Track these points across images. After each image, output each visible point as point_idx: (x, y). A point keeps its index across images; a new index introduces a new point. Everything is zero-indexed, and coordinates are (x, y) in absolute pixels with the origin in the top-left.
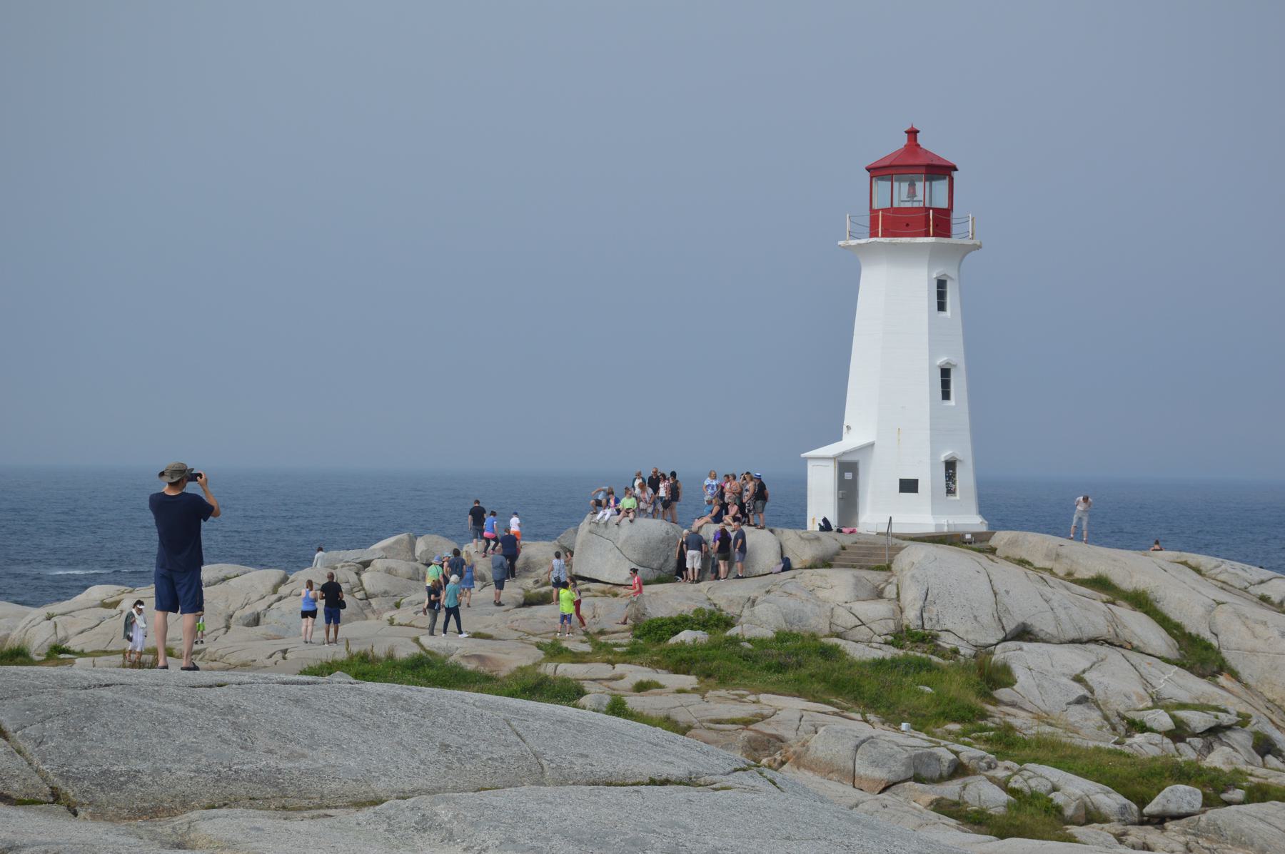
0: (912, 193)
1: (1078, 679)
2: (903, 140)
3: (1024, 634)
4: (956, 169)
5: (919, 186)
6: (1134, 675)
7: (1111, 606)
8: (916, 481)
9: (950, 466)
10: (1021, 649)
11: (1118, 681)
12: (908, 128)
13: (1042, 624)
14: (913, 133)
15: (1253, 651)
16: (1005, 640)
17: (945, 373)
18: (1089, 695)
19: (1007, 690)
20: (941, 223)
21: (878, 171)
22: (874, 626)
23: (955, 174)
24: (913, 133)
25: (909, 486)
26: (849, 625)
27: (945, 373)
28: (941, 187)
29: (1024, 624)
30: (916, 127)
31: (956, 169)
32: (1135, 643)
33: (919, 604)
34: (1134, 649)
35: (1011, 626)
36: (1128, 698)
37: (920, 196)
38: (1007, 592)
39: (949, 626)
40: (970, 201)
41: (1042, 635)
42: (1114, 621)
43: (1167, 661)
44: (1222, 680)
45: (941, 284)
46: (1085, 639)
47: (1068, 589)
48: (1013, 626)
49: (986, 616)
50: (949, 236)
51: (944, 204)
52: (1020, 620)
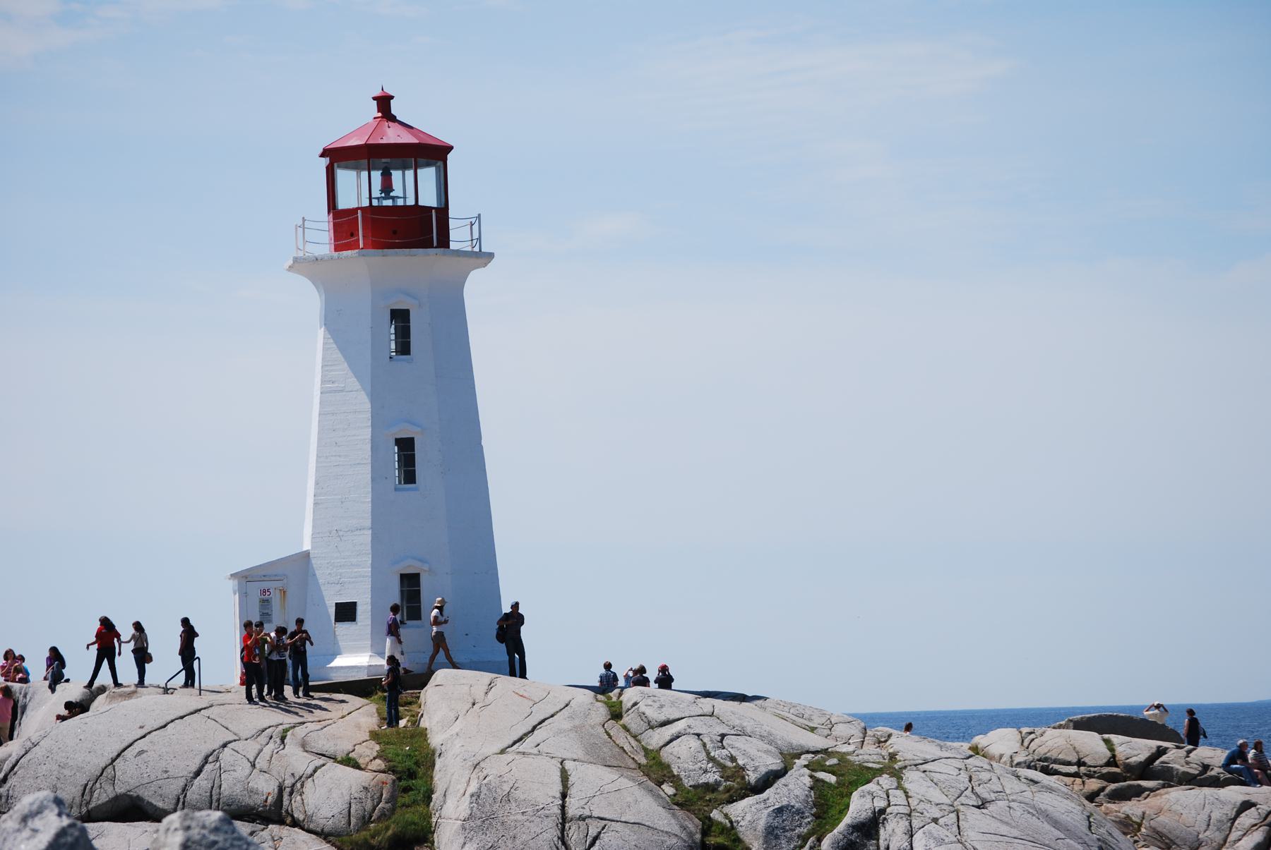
0: (387, 187)
2: (373, 110)
4: (449, 148)
5: (396, 175)
8: (354, 604)
12: (378, 93)
14: (384, 102)
17: (406, 447)
24: (384, 102)
25: (346, 612)
27: (406, 447)
28: (428, 175)
29: (125, 796)
30: (390, 92)
35: (102, 796)
37: (397, 191)
43: (323, 835)
48: (104, 799)
52: (120, 789)
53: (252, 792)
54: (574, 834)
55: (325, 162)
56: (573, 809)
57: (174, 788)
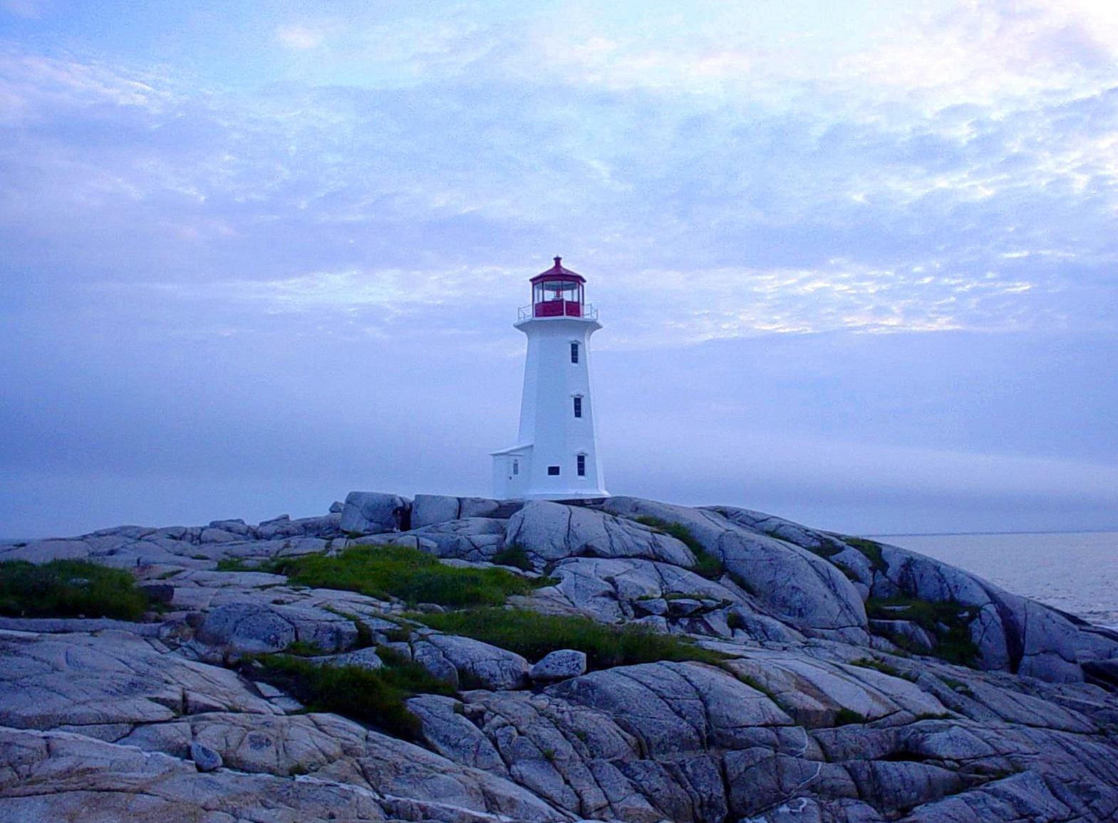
0: (558, 295)
1: (610, 580)
2: (553, 264)
3: (589, 552)
6: (657, 576)
7: (656, 535)
9: (581, 459)
10: (577, 561)
11: (641, 580)
12: (555, 256)
13: (601, 544)
14: (558, 260)
15: (744, 560)
16: (571, 556)
17: (578, 401)
18: (611, 588)
19: (551, 588)
20: (574, 309)
21: (535, 281)
22: (482, 549)
23: (585, 285)
24: (558, 260)
25: (554, 471)
26: (468, 549)
27: (578, 401)
30: (560, 256)
31: (584, 281)
32: (665, 557)
33: (514, 533)
34: (665, 561)
35: (576, 546)
36: (643, 590)
38: (579, 525)
39: (532, 548)
40: (592, 299)
41: (599, 553)
42: (655, 544)
43: (686, 568)
44: (724, 580)
45: (575, 348)
46: (631, 555)
47: (630, 525)
48: (577, 547)
49: (559, 542)
50: (579, 316)
51: (576, 300)
52: (584, 542)
53: (638, 545)
54: (821, 570)
55: (531, 284)
56: (809, 559)
57: (606, 541)
